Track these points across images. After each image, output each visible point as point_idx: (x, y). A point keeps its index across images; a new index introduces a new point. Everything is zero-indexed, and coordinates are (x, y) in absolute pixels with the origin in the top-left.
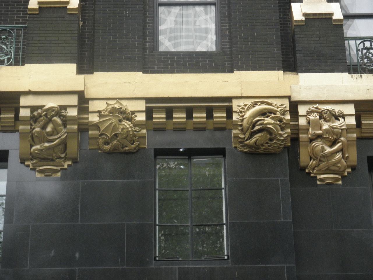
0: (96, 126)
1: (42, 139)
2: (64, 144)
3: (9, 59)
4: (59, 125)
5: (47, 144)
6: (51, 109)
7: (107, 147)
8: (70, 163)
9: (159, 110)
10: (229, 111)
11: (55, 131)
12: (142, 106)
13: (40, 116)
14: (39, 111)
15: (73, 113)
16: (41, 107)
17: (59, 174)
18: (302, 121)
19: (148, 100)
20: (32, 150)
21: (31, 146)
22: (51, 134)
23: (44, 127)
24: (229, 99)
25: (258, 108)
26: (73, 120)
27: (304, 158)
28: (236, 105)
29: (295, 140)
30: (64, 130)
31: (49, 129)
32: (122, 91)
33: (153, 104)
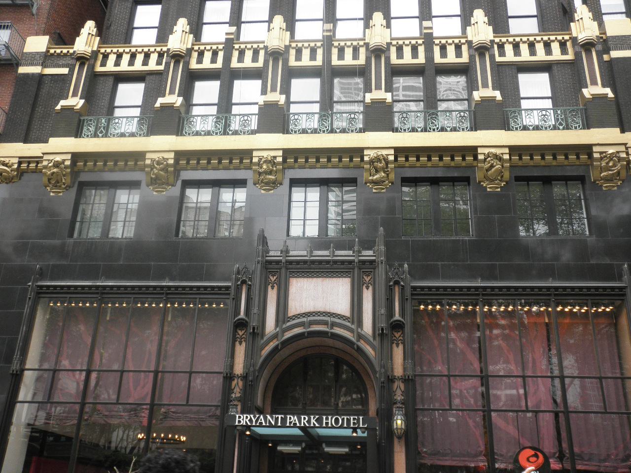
1: (608, 169)
2: (618, 173)
3: (579, 126)
4: (617, 162)
5: (610, 172)
6: (613, 153)
8: (621, 182)
11: (614, 165)
13: (605, 157)
14: (604, 154)
15: (624, 155)
16: (605, 152)
17: (616, 188)
20: (602, 175)
21: (601, 173)
22: (612, 167)
23: (607, 163)
26: (624, 159)
30: (619, 165)
31: (611, 164)
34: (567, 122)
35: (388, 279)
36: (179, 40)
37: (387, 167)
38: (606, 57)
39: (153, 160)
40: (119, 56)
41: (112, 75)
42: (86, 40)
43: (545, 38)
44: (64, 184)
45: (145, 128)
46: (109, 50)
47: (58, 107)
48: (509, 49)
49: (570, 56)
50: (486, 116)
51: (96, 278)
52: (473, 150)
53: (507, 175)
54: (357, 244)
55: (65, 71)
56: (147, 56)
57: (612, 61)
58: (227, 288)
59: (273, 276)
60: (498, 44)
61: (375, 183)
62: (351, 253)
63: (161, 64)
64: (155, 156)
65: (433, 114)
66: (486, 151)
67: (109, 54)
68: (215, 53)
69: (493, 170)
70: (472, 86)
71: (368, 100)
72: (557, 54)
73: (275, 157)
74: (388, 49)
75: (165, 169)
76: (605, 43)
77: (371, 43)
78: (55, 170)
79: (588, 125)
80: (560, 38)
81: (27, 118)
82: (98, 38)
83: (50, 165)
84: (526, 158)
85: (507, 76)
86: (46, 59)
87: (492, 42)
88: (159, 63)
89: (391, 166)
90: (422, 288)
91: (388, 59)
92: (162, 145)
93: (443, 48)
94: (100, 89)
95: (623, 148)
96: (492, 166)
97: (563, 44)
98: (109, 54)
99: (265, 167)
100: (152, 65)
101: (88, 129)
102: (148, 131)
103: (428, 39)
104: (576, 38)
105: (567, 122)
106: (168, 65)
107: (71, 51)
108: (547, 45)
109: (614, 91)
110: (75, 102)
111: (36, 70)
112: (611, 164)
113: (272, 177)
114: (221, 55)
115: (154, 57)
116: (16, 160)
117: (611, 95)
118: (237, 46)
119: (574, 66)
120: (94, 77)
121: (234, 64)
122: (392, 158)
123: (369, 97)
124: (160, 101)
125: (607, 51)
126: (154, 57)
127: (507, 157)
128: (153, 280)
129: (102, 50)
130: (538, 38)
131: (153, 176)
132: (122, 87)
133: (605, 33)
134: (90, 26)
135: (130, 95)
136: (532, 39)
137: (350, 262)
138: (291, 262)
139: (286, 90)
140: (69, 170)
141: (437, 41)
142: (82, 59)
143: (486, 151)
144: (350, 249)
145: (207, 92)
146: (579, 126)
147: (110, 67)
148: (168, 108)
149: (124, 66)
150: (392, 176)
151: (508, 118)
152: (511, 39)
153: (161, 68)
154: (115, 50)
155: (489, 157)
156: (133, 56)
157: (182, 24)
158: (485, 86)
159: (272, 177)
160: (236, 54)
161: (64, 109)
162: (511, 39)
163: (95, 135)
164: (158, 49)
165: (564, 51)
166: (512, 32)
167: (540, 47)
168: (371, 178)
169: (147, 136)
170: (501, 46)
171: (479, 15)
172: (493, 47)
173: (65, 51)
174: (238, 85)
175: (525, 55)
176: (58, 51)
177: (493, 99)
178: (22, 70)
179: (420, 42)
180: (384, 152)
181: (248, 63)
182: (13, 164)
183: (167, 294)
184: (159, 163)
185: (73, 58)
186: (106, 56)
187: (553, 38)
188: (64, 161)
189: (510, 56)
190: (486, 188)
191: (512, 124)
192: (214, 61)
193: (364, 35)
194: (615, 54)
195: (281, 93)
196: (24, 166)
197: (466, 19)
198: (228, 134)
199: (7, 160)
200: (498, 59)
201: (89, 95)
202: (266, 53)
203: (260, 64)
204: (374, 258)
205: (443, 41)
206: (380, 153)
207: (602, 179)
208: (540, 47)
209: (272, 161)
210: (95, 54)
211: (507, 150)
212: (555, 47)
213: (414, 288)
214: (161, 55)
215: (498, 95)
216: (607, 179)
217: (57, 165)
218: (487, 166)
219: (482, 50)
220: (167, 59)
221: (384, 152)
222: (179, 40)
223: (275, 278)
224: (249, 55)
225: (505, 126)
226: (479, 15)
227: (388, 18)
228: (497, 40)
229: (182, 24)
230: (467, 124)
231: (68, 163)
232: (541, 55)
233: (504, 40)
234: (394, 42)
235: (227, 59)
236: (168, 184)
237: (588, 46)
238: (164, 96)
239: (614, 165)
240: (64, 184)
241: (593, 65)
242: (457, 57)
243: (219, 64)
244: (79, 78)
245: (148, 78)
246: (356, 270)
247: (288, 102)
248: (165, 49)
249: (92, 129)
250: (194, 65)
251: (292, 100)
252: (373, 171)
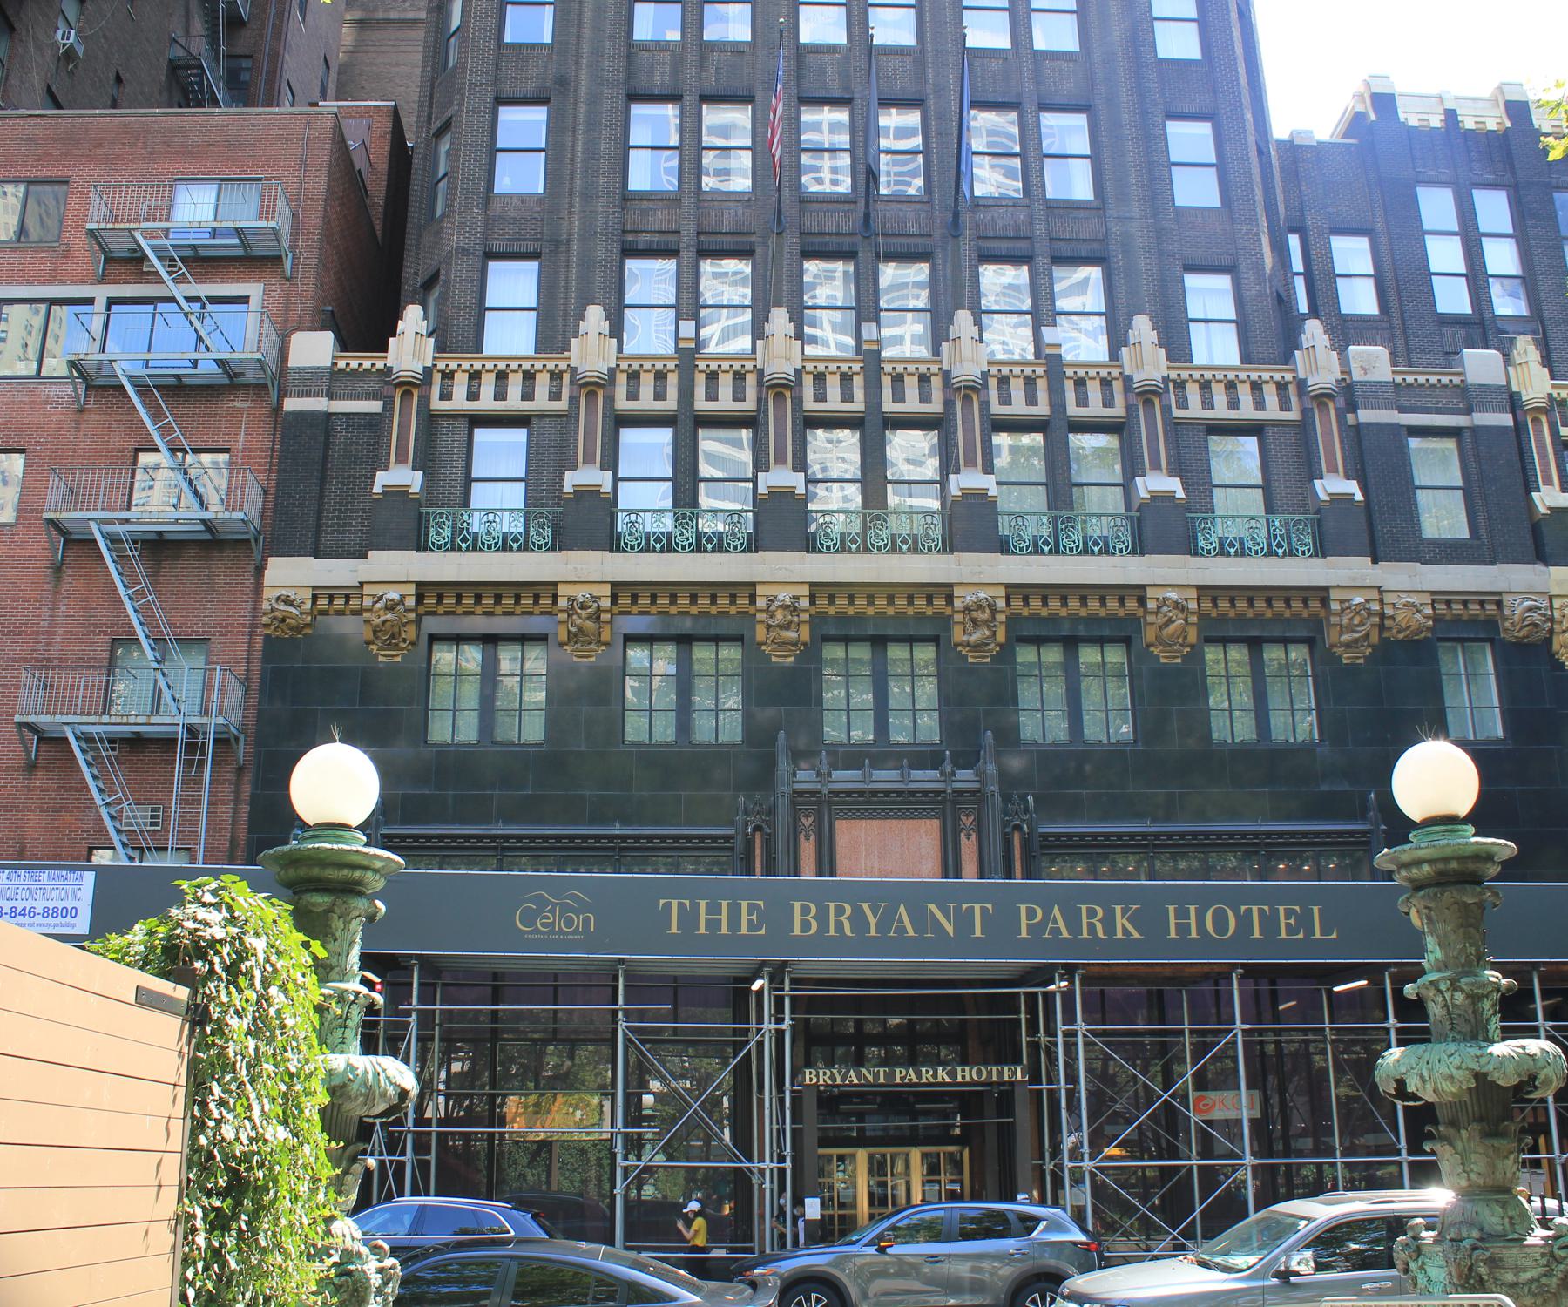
0: (1393, 618)
2: (1367, 635)
7: (1401, 636)
9: (1440, 601)
10: (1499, 604)
11: (1362, 624)
12: (1427, 599)
15: (1376, 607)
18: (1557, 614)
19: (1433, 593)
24: (1500, 593)
25: (1527, 603)
27: (1556, 647)
28: (1507, 599)
29: (1551, 631)
32: (1409, 585)
33: (1437, 596)
34: (1289, 543)
35: (1005, 824)
36: (591, 350)
37: (994, 618)
38: (1350, 418)
39: (572, 600)
40: (475, 376)
41: (463, 416)
42: (411, 345)
43: (1254, 376)
44: (404, 640)
45: (547, 533)
46: (453, 365)
47: (377, 489)
48: (1193, 394)
49: (1293, 415)
50: (1157, 528)
51: (486, 819)
52: (1139, 592)
53: (1192, 636)
54: (948, 761)
55: (375, 406)
56: (529, 377)
57: (1358, 427)
58: (727, 839)
59: (807, 816)
60: (1174, 382)
61: (976, 647)
62: (936, 774)
64: (581, 593)
65: (1069, 519)
66: (1160, 594)
67: (453, 372)
68: (661, 376)
69: (1172, 627)
70: (1132, 469)
72: (1272, 411)
73: (796, 598)
74: (985, 386)
75: (596, 617)
76: (1350, 394)
77: (954, 374)
78: (389, 616)
79: (1321, 551)
80: (1277, 376)
81: (314, 506)
82: (432, 340)
83: (378, 606)
84: (1224, 604)
85: (1188, 448)
86: (333, 381)
87: (1166, 379)
88: (555, 396)
89: (1001, 617)
90: (1058, 836)
91: (985, 405)
92: (584, 570)
93: (1080, 383)
94: (443, 444)
95: (1375, 595)
96: (1170, 621)
97: (1282, 387)
98: (453, 372)
99: (779, 615)
100: (541, 401)
101: (438, 534)
102: (554, 545)
103: (1053, 364)
104: (1305, 381)
105: (1289, 543)
106: (574, 400)
107: (380, 365)
108: (1256, 387)
109: (1364, 489)
110: (401, 476)
111: (318, 404)
112: (1356, 621)
113: (790, 635)
114: (673, 379)
115: (543, 382)
116: (308, 594)
117: (1359, 497)
118: (702, 365)
119: (1303, 430)
120: (431, 420)
121: (701, 404)
122: (1001, 604)
124: (572, 480)
125: (1353, 407)
126: (542, 384)
127: (1193, 605)
128: (593, 821)
129: (441, 365)
130: (1243, 375)
131: (573, 629)
132: (481, 435)
133: (1349, 373)
134: (413, 319)
135: (500, 455)
136: (1231, 375)
137: (937, 793)
138: (836, 793)
140: (412, 616)
141: (1069, 372)
142: (407, 386)
143: (1160, 594)
144: (934, 768)
145: (648, 449)
147: (459, 401)
148: (581, 493)
149: (487, 401)
150: (1001, 636)
151: (1195, 533)
152: (1196, 375)
153: (563, 404)
154: (466, 365)
155: (1164, 604)
156: (502, 377)
157: (595, 317)
158: (1156, 466)
159: (790, 635)
160: (700, 379)
161: (388, 492)
162: (1196, 375)
163: (454, 548)
164: (551, 365)
165: (1284, 405)
166: (1199, 358)
167: (1245, 395)
168: (965, 638)
169: (554, 549)
170: (1180, 385)
171: (1143, 328)
172: (1168, 391)
173: (367, 364)
174: (710, 443)
175: (1221, 411)
176: (354, 364)
177: (1169, 496)
178: (292, 404)
179: (1040, 371)
180: (992, 592)
181: (725, 402)
182: (303, 601)
183: (622, 849)
184: (583, 607)
185: (387, 383)
186: (448, 376)
187: (1266, 376)
188: (403, 597)
189: (1195, 410)
190: (1157, 657)
191: (1202, 543)
192: (660, 395)
193: (936, 352)
194: (1365, 416)
195: (795, 469)
196: (323, 602)
197: (1117, 338)
198: (706, 550)
199: (292, 594)
200: (1177, 413)
201: (426, 461)
202: (760, 383)
203: (749, 405)
204: (977, 785)
205: (1081, 372)
206: (982, 596)
207: (1342, 645)
208: (1245, 395)
209: (793, 609)
210: (428, 372)
211: (1193, 594)
212: (1271, 396)
213: (1045, 836)
214: (556, 376)
215: (1175, 485)
216: (1349, 645)
217: (391, 607)
218: (1161, 620)
219: (1148, 396)
220: (571, 391)
221: (992, 592)
222: (591, 350)
223: (811, 820)
224: (725, 382)
225: (1190, 547)
226: (1143, 328)
227: (978, 314)
228: (1173, 375)
229: (595, 317)
230: (1127, 538)
231: (411, 602)
232: (1247, 411)
233: (1185, 375)
234: (994, 370)
235: (686, 393)
236: (600, 643)
237: (1322, 398)
238: (574, 468)
239: (1362, 624)
240: (404, 640)
241: (1329, 435)
242: (1105, 405)
244: (405, 425)
245: (534, 422)
246: (948, 805)
248: (563, 365)
249: (447, 533)
252: (969, 626)
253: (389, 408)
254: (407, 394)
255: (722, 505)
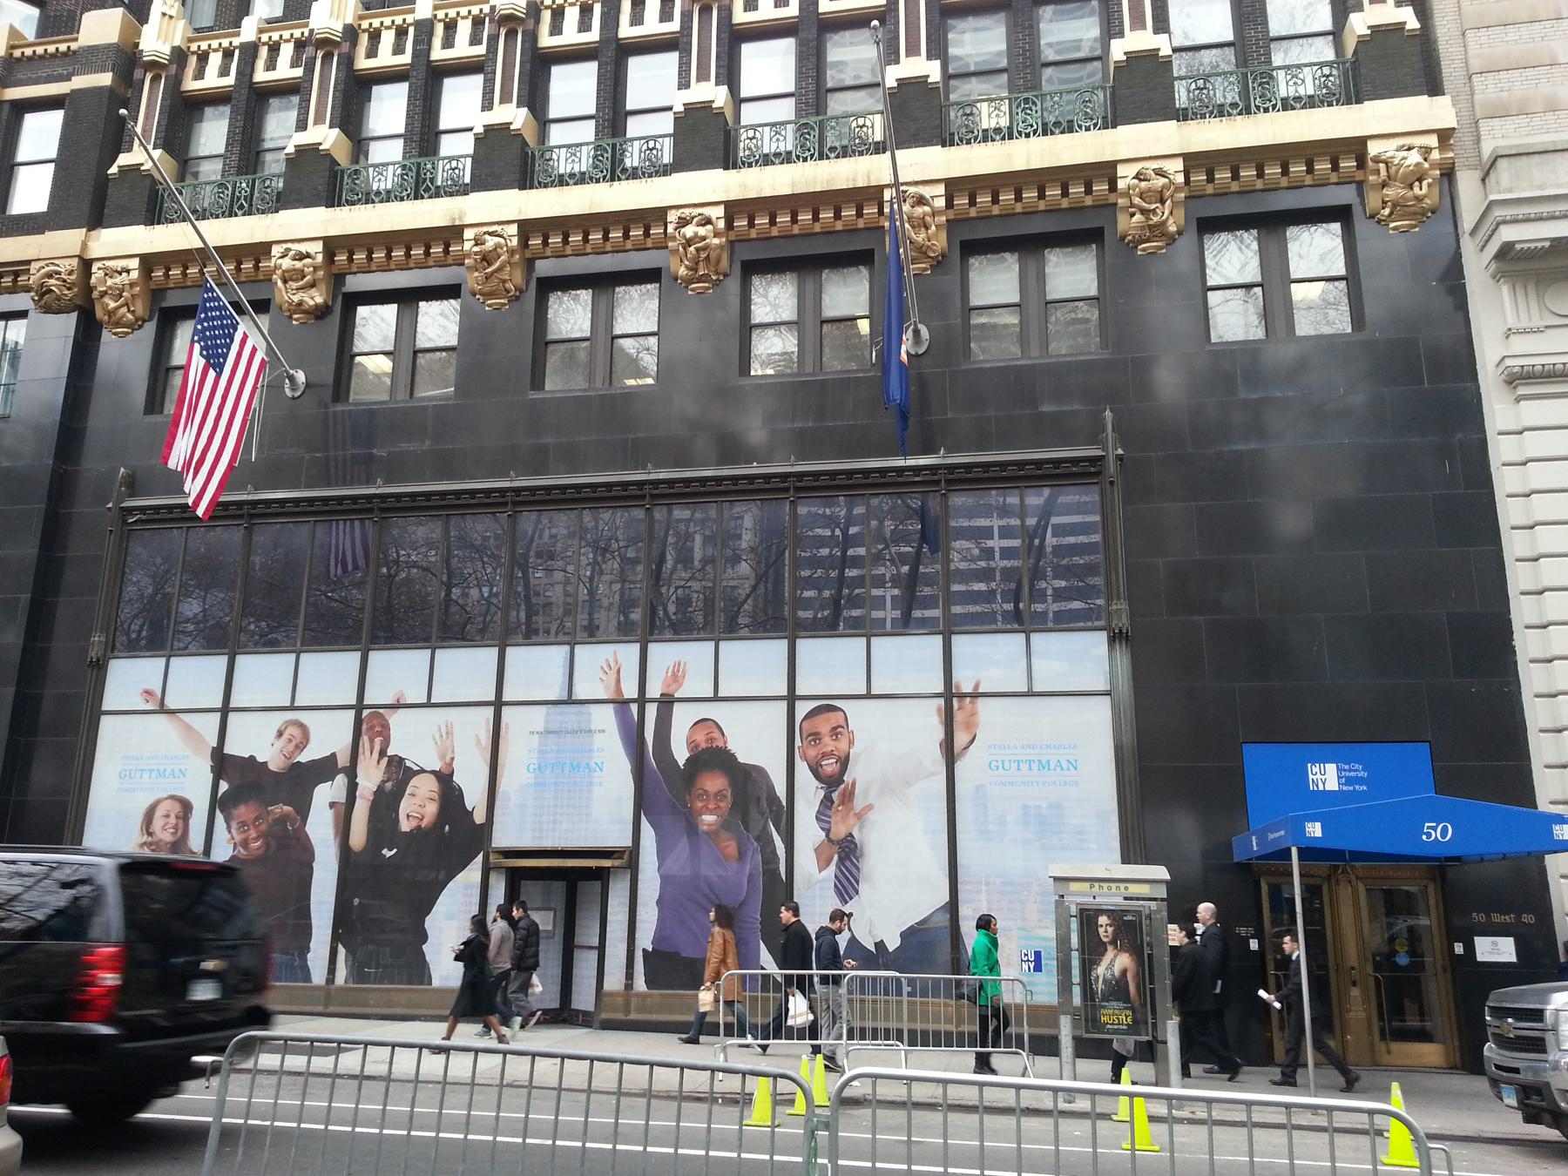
63: (480, 43)
71: (891, 82)
88: (475, 40)
106: (493, 39)
121: (626, 31)
123: (892, 75)
139: (730, 75)
142: (326, 44)
146: (1274, 107)
153: (481, 50)
192: (584, 26)
243: (594, 35)
247: (737, 100)
250: (546, 40)
251: (745, 92)
253: (309, 70)
254: (328, 57)
255: (650, 130)
